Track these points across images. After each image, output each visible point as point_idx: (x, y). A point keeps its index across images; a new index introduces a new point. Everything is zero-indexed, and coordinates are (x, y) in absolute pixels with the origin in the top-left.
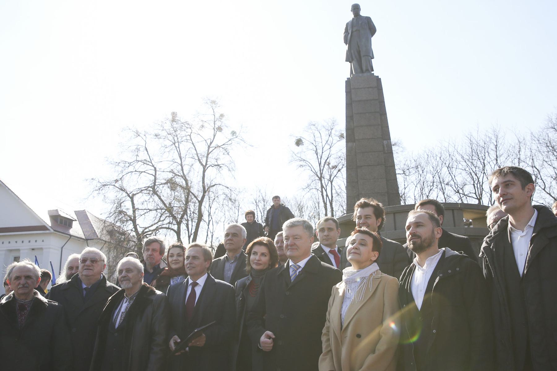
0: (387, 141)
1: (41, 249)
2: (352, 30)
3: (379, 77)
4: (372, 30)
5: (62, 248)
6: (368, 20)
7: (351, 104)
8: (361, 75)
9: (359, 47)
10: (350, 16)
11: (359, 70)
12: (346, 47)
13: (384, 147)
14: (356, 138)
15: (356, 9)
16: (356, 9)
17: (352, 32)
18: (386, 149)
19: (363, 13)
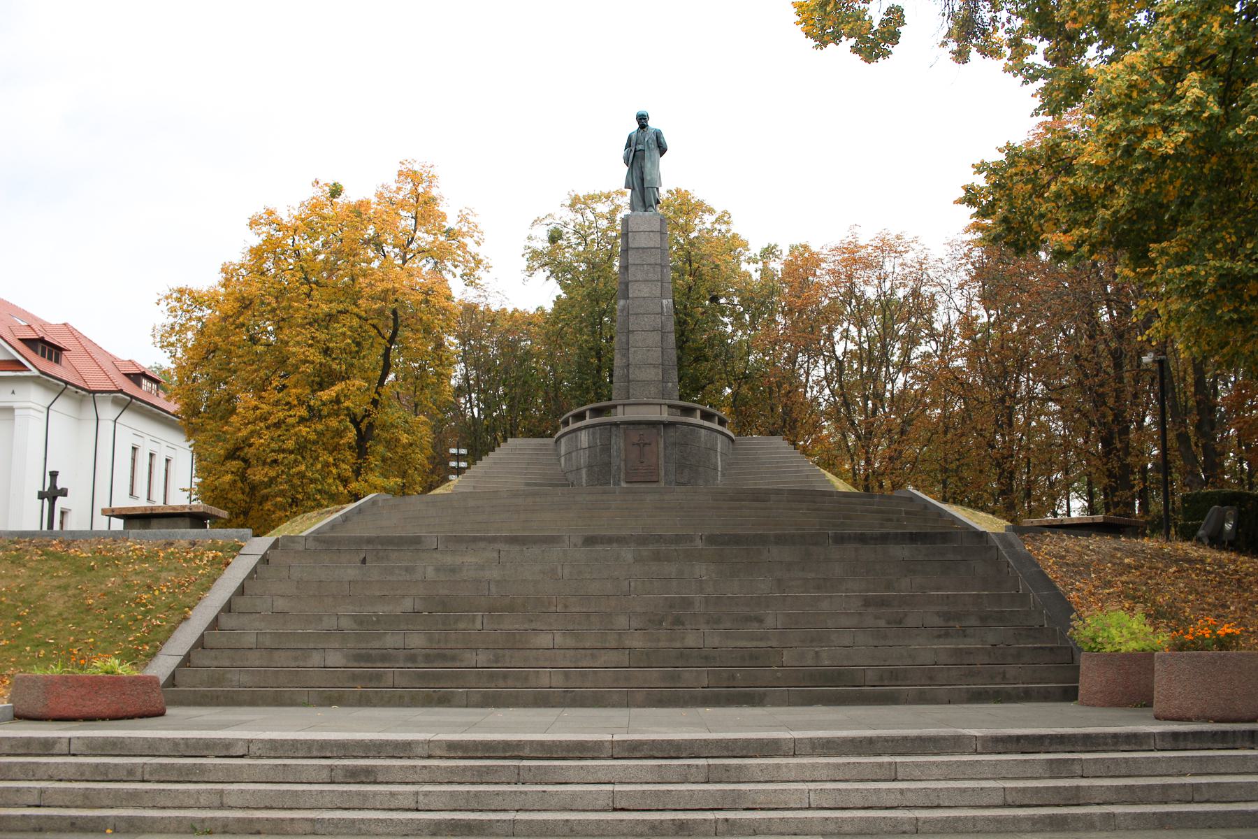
1: (11, 410)
4: (662, 150)
5: (48, 408)
6: (658, 136)
7: (627, 250)
8: (641, 213)
10: (635, 126)
11: (639, 203)
12: (626, 169)
13: (662, 308)
14: (630, 296)
15: (642, 120)
16: (642, 120)
17: (635, 151)
18: (665, 310)
19: (652, 124)
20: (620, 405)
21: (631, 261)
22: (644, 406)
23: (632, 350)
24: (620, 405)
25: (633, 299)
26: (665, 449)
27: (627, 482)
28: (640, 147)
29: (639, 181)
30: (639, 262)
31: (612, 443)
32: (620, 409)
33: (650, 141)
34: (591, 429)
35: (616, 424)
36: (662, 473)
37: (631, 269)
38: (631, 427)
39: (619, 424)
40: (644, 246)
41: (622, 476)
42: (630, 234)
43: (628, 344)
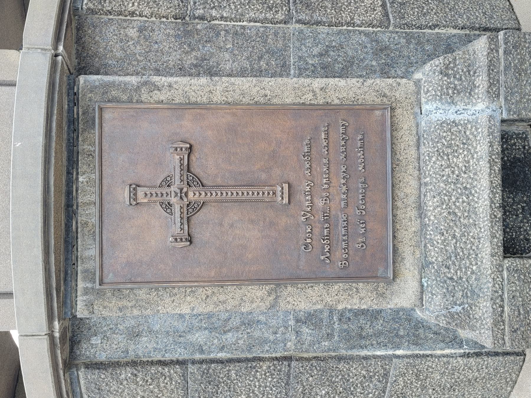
26: (211, 73)
31: (180, 354)
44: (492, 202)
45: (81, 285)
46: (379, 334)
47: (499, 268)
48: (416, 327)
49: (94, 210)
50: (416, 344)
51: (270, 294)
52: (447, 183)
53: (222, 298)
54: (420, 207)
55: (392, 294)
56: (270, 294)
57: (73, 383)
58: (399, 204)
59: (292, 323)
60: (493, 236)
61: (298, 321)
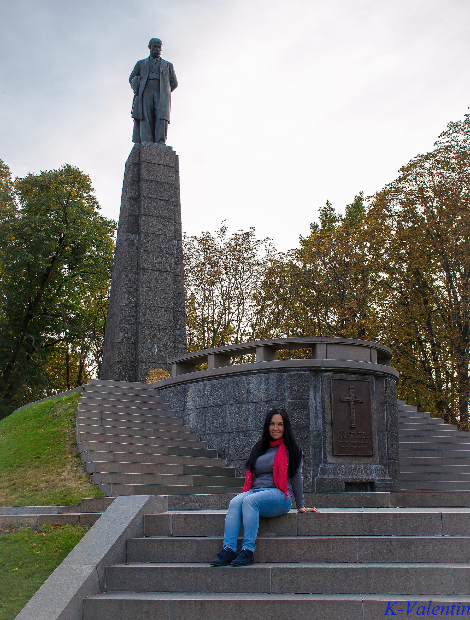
0: (178, 242)
2: (149, 76)
3: (176, 154)
4: (174, 85)
9: (154, 103)
10: (146, 54)
11: (150, 136)
17: (148, 79)
19: (163, 55)
20: (321, 343)
21: (143, 193)
22: (352, 348)
23: (142, 290)
24: (321, 343)
25: (145, 234)
27: (335, 456)
28: (153, 76)
29: (149, 111)
30: (152, 196)
32: (320, 350)
33: (165, 73)
34: (273, 376)
35: (316, 371)
36: (376, 444)
37: (144, 202)
38: (338, 376)
39: (323, 371)
40: (158, 179)
41: (329, 447)
42: (144, 164)
43: (137, 282)
44: (357, 479)
45: (330, 374)
46: (315, 454)
47: (342, 481)
48: (317, 465)
49: (346, 378)
50: (313, 465)
51: (329, 422)
52: (358, 469)
53: (328, 409)
54: (350, 464)
55: (330, 455)
56: (329, 422)
57: (304, 371)
58: (351, 458)
59: (318, 429)
60: (349, 479)
61: (319, 430)
